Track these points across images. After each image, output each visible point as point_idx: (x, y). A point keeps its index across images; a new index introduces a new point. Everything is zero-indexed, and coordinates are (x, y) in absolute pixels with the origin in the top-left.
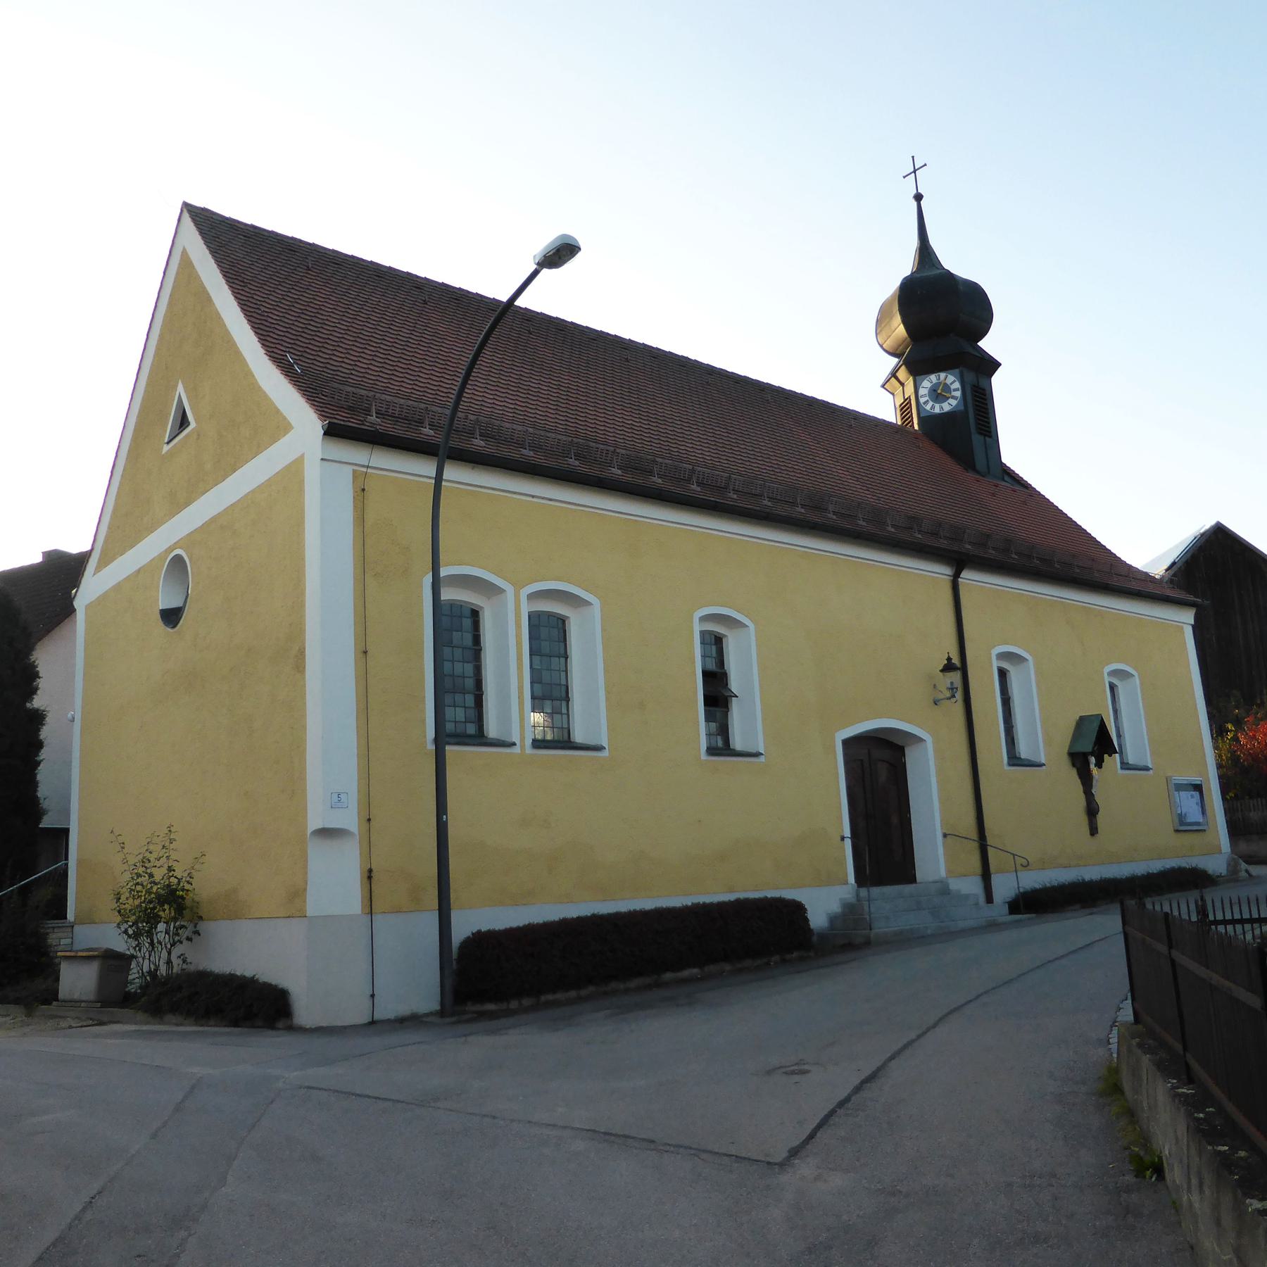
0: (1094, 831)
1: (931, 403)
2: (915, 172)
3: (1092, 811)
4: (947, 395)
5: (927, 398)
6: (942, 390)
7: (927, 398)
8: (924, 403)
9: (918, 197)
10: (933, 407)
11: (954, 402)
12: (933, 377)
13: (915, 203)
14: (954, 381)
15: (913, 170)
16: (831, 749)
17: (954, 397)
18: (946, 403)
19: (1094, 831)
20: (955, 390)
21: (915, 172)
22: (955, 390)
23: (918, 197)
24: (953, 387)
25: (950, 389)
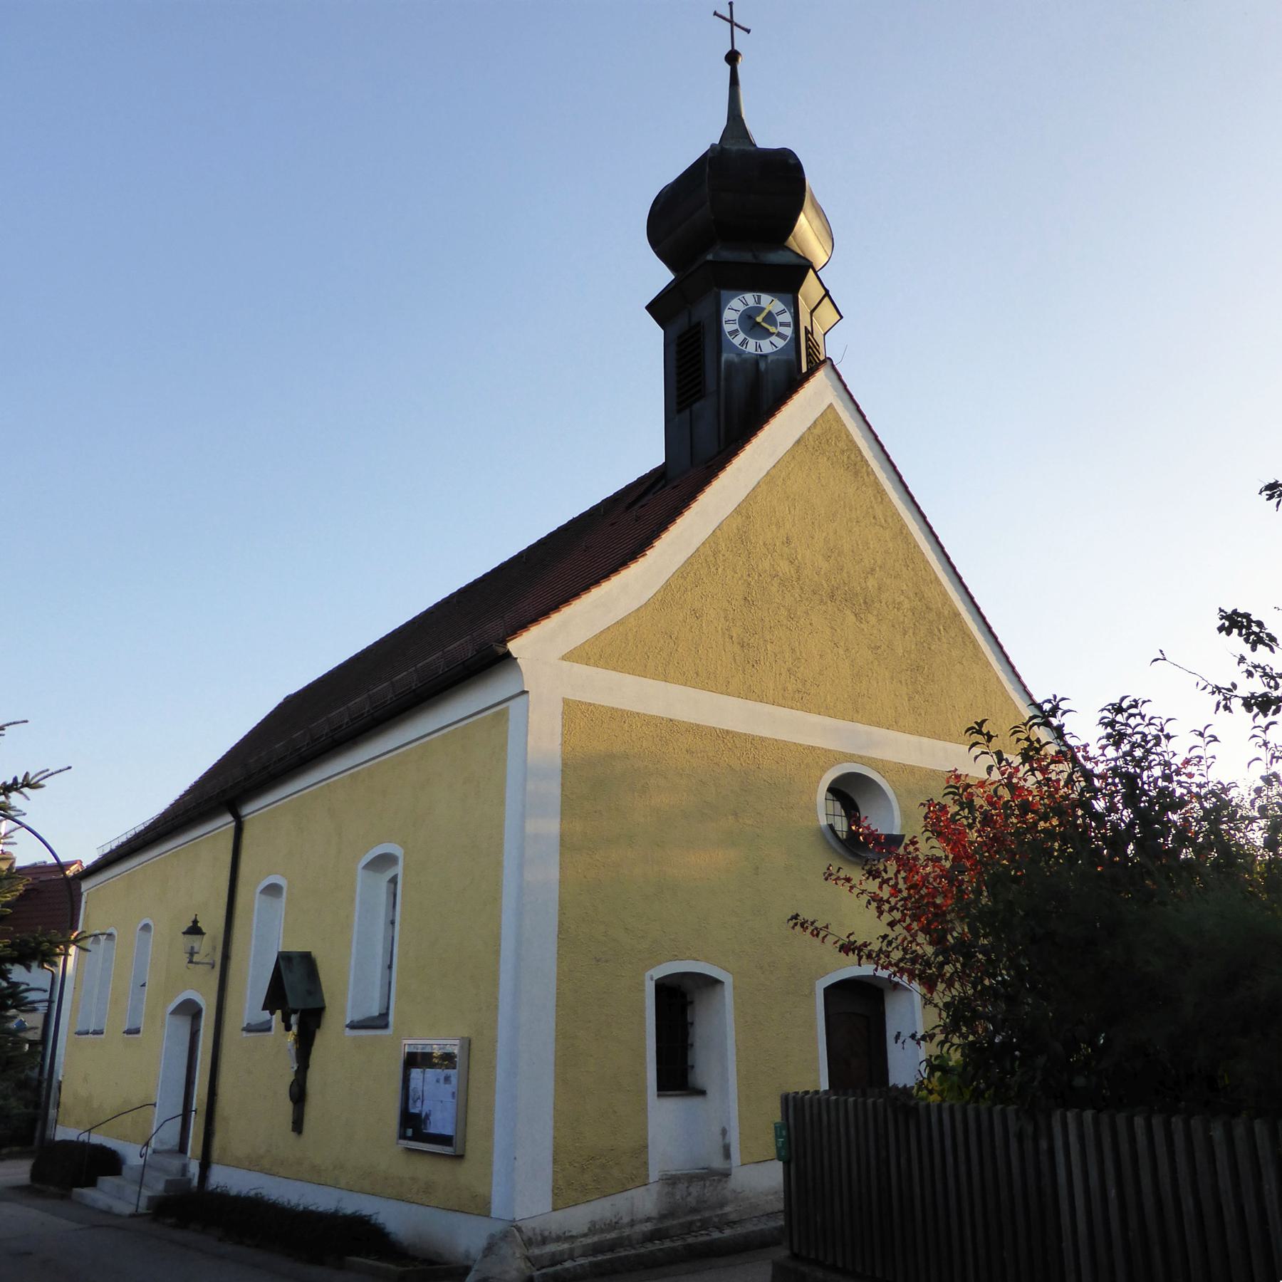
0: (298, 1126)
1: (741, 336)
2: (731, 21)
3: (299, 1094)
4: (772, 329)
5: (736, 326)
6: (764, 320)
7: (736, 326)
8: (731, 333)
9: (732, 58)
10: (744, 342)
11: (781, 343)
12: (750, 298)
13: (728, 67)
14: (783, 312)
15: (729, 24)
16: (640, 988)
17: (779, 335)
18: (767, 341)
19: (298, 1126)
20: (782, 324)
21: (731, 21)
22: (782, 324)
23: (732, 58)
24: (780, 319)
25: (775, 320)
